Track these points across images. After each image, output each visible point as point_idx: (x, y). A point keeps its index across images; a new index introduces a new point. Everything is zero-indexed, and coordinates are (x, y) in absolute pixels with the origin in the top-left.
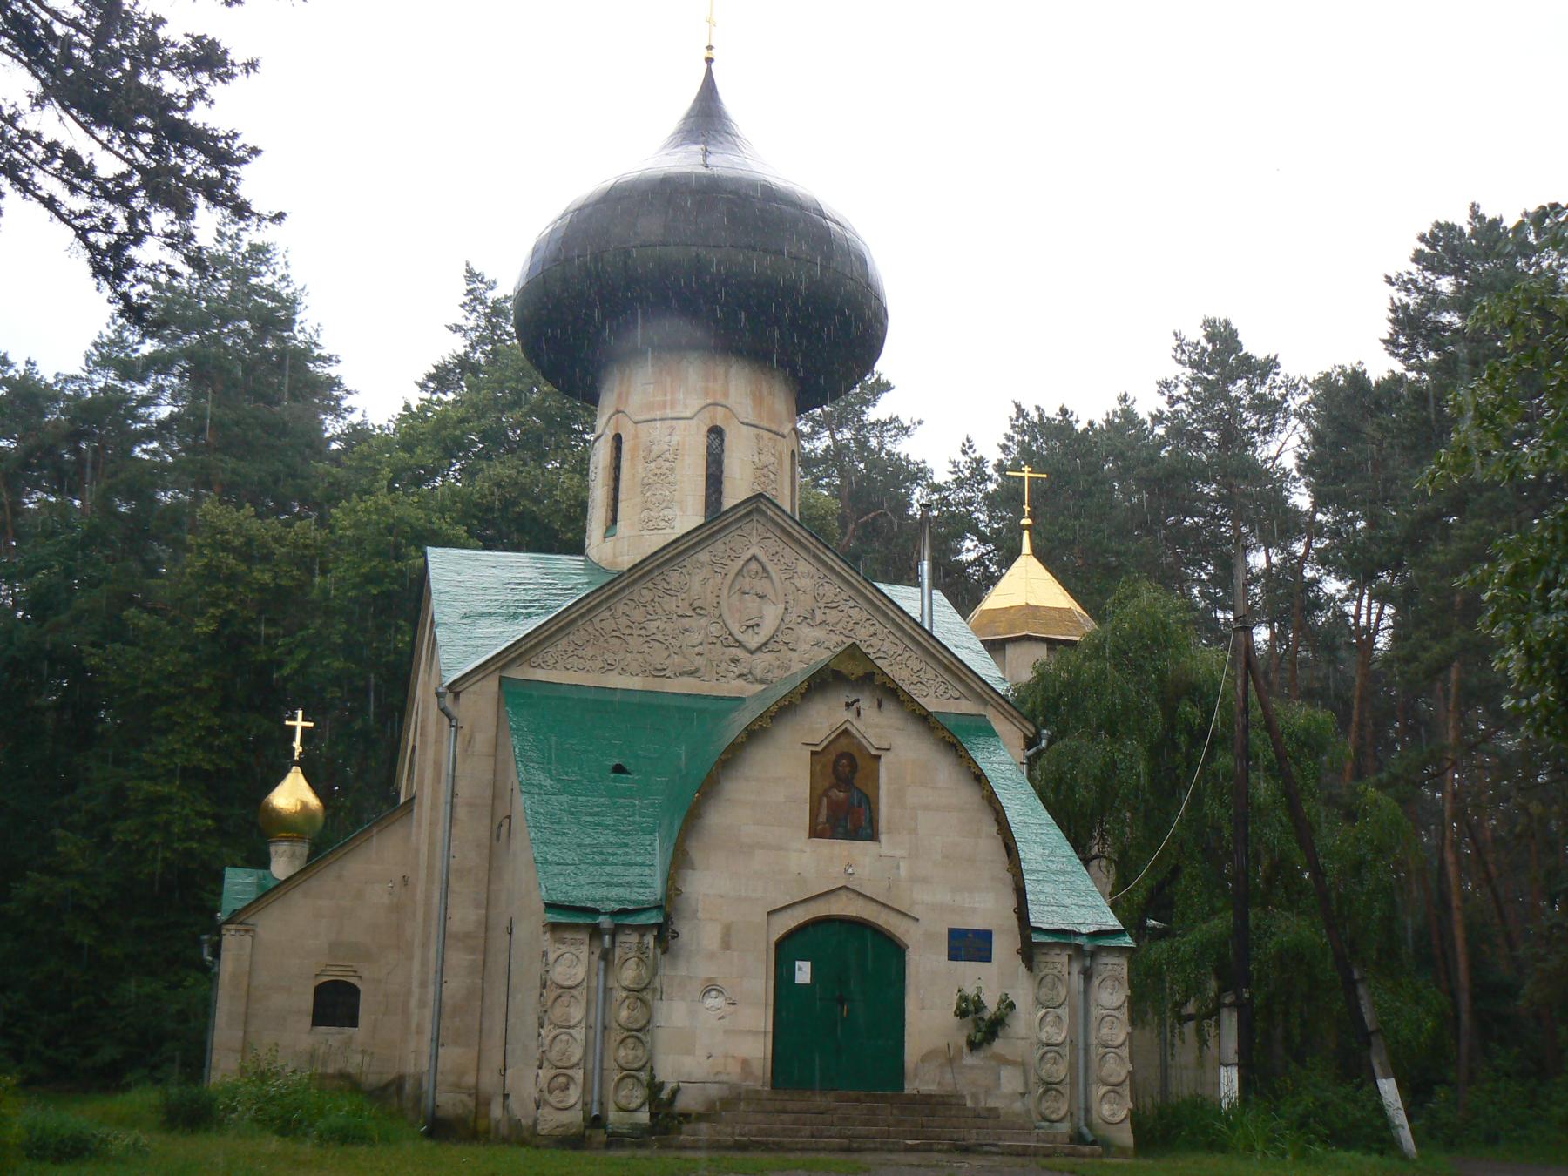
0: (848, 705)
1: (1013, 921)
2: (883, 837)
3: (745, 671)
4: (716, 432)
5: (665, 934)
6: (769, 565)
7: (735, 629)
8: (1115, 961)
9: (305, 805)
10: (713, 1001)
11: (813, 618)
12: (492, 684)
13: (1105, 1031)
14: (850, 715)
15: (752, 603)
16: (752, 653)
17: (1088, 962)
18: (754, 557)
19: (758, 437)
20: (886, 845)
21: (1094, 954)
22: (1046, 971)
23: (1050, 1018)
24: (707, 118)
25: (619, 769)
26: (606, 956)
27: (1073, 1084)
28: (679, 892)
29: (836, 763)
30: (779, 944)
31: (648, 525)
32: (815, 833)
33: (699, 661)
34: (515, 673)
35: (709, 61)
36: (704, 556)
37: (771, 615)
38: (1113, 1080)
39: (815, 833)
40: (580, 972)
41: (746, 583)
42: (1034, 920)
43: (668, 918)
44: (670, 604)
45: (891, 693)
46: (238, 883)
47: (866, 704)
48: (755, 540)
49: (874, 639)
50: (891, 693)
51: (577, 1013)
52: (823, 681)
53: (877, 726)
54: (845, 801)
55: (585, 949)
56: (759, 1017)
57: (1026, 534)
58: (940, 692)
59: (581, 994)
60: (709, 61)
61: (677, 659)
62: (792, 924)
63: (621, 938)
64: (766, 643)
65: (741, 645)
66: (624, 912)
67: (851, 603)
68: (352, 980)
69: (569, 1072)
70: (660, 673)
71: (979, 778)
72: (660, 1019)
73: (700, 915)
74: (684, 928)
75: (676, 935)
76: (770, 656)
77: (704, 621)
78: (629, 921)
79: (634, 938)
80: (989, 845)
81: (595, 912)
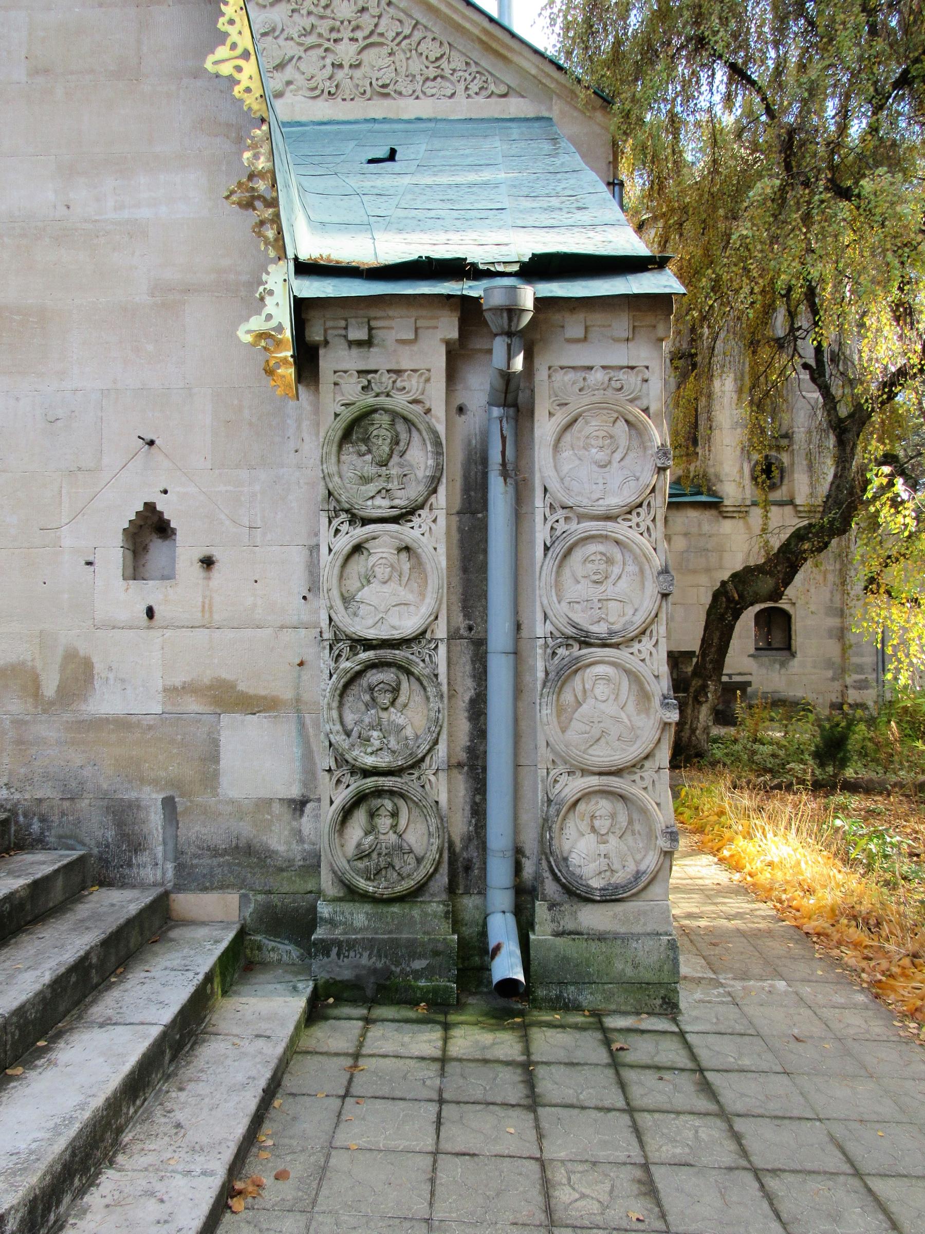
8: (619, 356)
13: (577, 590)
38: (602, 756)
49: (366, 16)
58: (474, 88)
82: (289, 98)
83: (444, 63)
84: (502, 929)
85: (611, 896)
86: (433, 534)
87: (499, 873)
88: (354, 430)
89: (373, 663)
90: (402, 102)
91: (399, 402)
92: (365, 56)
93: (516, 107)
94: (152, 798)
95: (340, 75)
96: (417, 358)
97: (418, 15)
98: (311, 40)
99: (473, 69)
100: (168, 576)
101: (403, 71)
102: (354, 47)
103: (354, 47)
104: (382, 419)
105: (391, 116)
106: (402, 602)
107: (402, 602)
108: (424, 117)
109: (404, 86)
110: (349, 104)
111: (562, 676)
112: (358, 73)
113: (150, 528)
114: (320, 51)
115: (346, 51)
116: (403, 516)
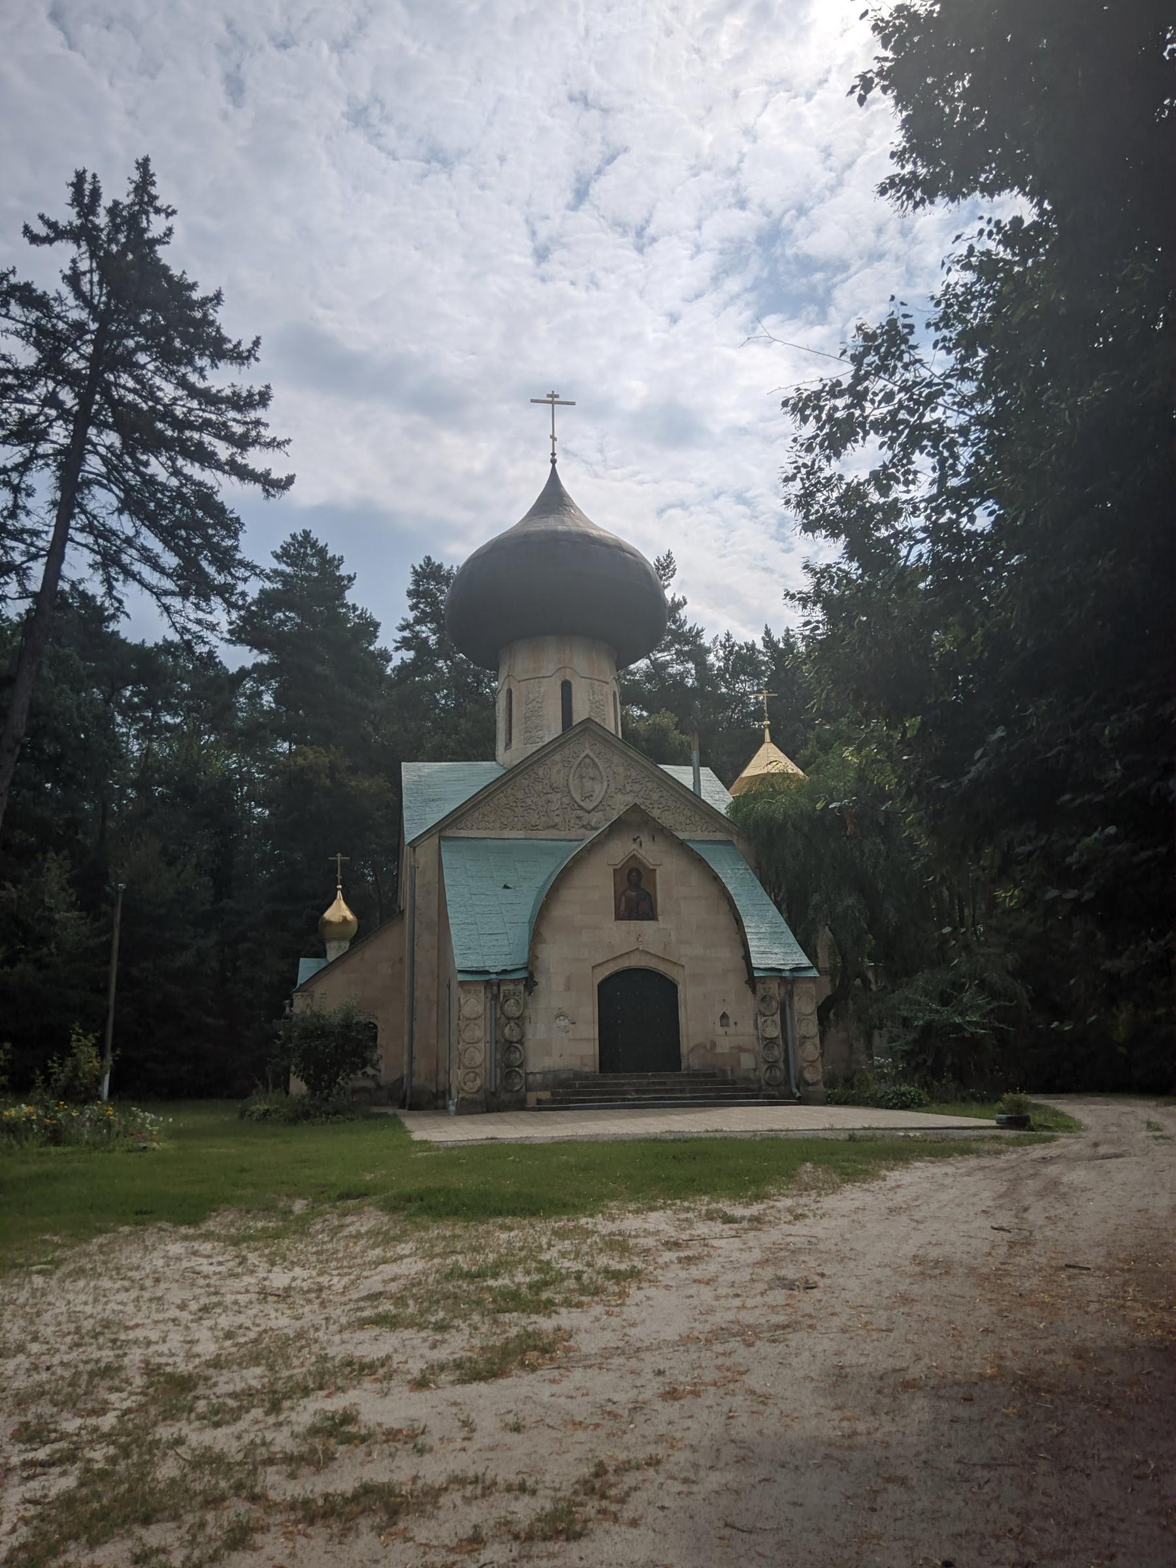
0: (635, 840)
1: (743, 963)
2: (660, 918)
4: (566, 687)
5: (530, 984)
6: (596, 760)
7: (578, 799)
9: (345, 919)
10: (563, 1023)
12: (435, 839)
14: (635, 846)
15: (588, 784)
17: (789, 987)
18: (587, 756)
19: (592, 686)
20: (662, 923)
21: (794, 981)
23: (769, 1022)
24: (553, 498)
25: (506, 887)
26: (495, 997)
27: (786, 1061)
28: (537, 958)
30: (602, 986)
31: (527, 741)
32: (618, 917)
33: (557, 820)
34: (449, 833)
35: (554, 462)
36: (557, 757)
37: (599, 790)
38: (810, 1059)
39: (618, 917)
40: (480, 1009)
42: (756, 961)
43: (531, 975)
44: (539, 787)
45: (661, 832)
46: (307, 967)
47: (645, 838)
48: (587, 745)
50: (661, 832)
51: (479, 1033)
52: (617, 828)
53: (651, 852)
54: (636, 898)
55: (482, 995)
56: (590, 1030)
57: (767, 731)
59: (481, 1022)
60: (554, 462)
61: (543, 819)
62: (608, 973)
63: (503, 988)
64: (596, 807)
65: (581, 808)
66: (504, 972)
68: (373, 1021)
69: (477, 1070)
70: (534, 828)
71: (716, 878)
72: (529, 1035)
73: (552, 970)
74: (541, 979)
75: (536, 984)
77: (559, 795)
78: (508, 977)
79: (511, 987)
80: (724, 919)
81: (487, 973)
84: (795, 1090)
85: (814, 1084)
86: (777, 1018)
87: (793, 1081)
88: (763, 999)
89: (770, 1042)
93: (719, 836)
94: (729, 1068)
96: (774, 988)
100: (728, 1025)
106: (774, 1032)
107: (774, 1032)
111: (801, 1044)
113: (724, 1016)
116: (773, 1015)
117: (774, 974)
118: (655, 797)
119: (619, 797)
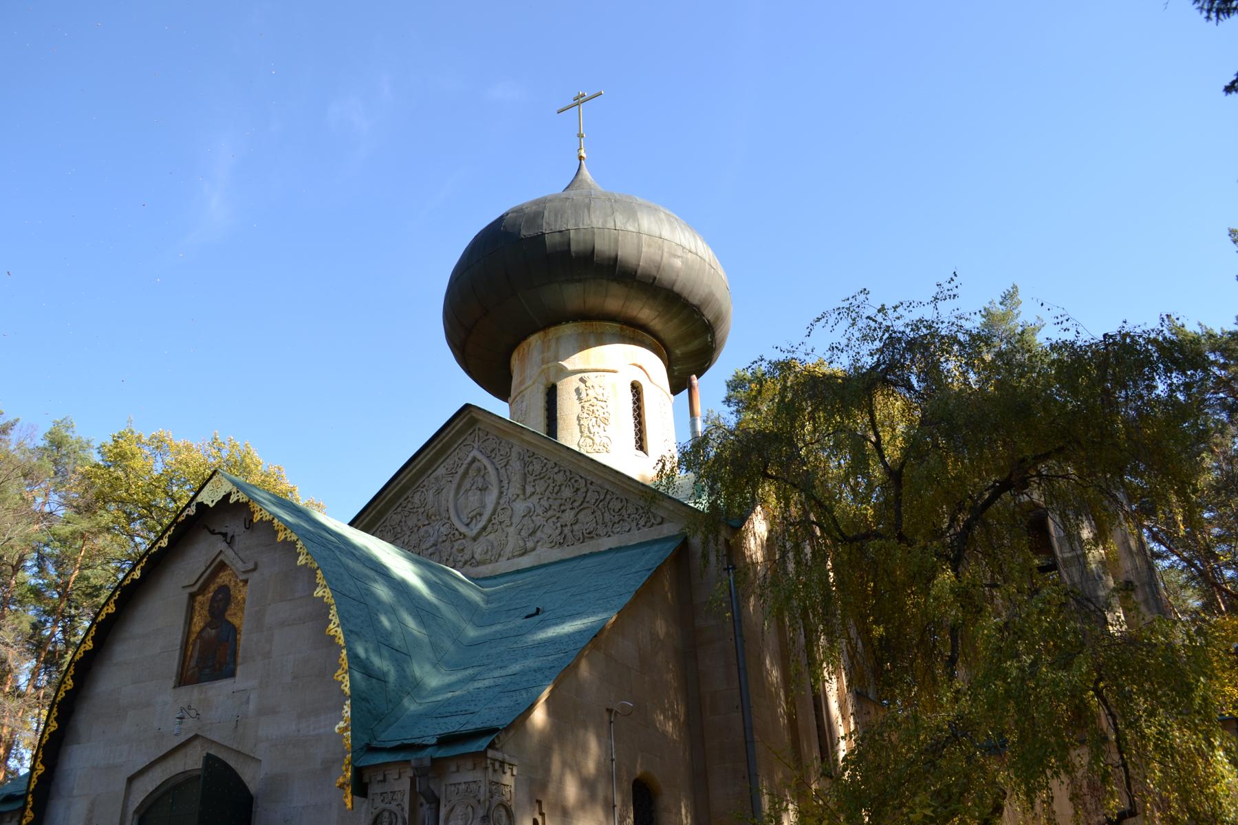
2: (239, 670)
3: (467, 557)
8: (470, 777)
11: (524, 494)
14: (222, 546)
15: (473, 499)
16: (475, 539)
22: (383, 806)
29: (213, 599)
36: (441, 471)
39: (183, 680)
41: (467, 484)
58: (642, 522)
64: (484, 528)
67: (556, 470)
73: (75, 792)
76: (491, 537)
82: (539, 550)
83: (623, 511)
90: (600, 541)
91: (393, 807)
92: (581, 516)
95: (566, 530)
97: (607, 487)
98: (550, 513)
99: (641, 511)
101: (600, 522)
102: (573, 512)
103: (573, 512)
104: (386, 814)
105: (595, 550)
108: (613, 546)
109: (601, 530)
110: (571, 548)
112: (576, 527)
114: (554, 519)
115: (568, 516)
117: (400, 757)
118: (567, 493)
119: (520, 507)
